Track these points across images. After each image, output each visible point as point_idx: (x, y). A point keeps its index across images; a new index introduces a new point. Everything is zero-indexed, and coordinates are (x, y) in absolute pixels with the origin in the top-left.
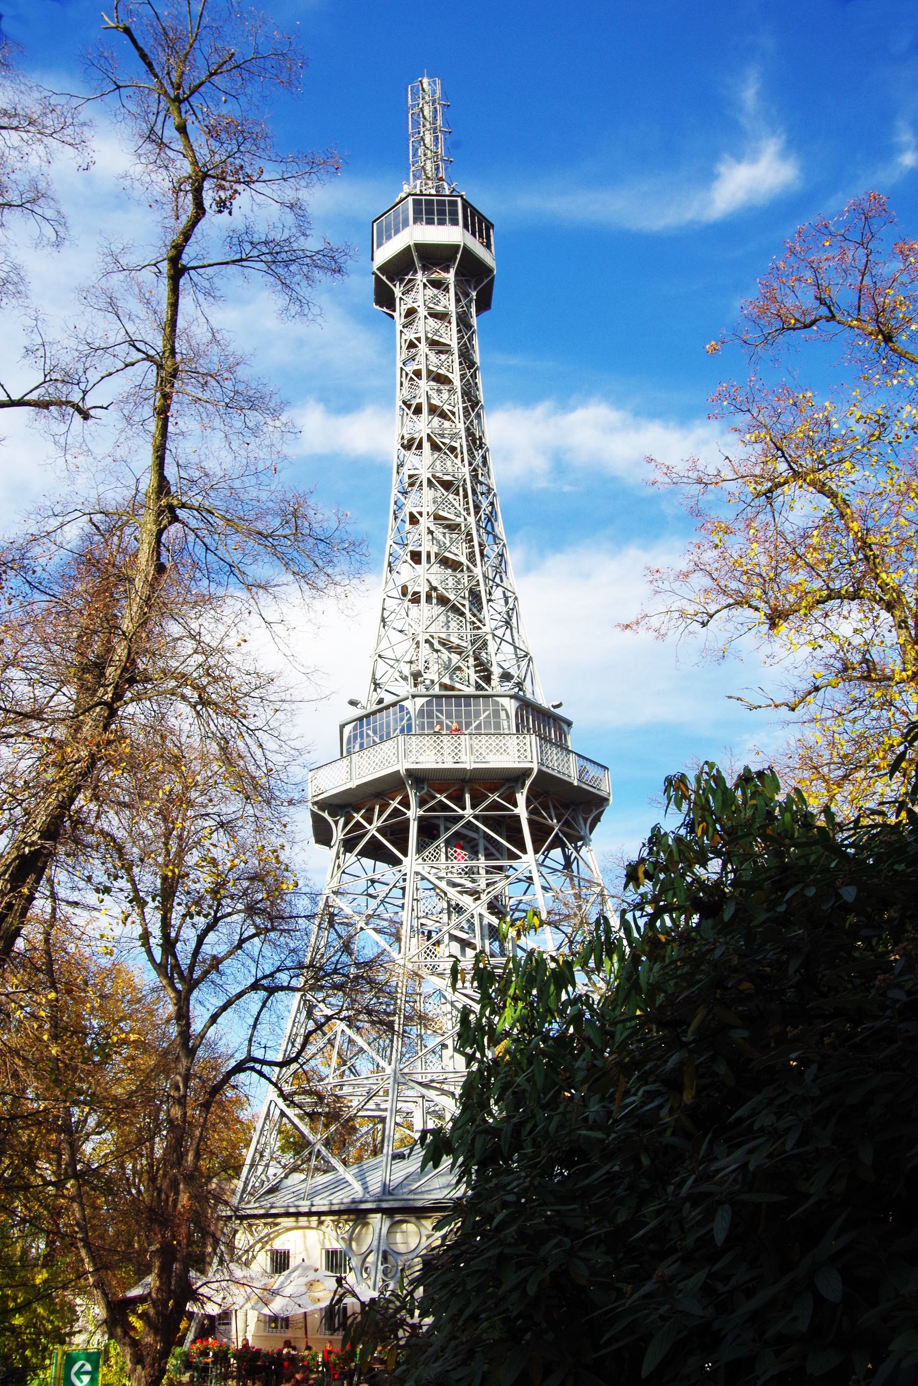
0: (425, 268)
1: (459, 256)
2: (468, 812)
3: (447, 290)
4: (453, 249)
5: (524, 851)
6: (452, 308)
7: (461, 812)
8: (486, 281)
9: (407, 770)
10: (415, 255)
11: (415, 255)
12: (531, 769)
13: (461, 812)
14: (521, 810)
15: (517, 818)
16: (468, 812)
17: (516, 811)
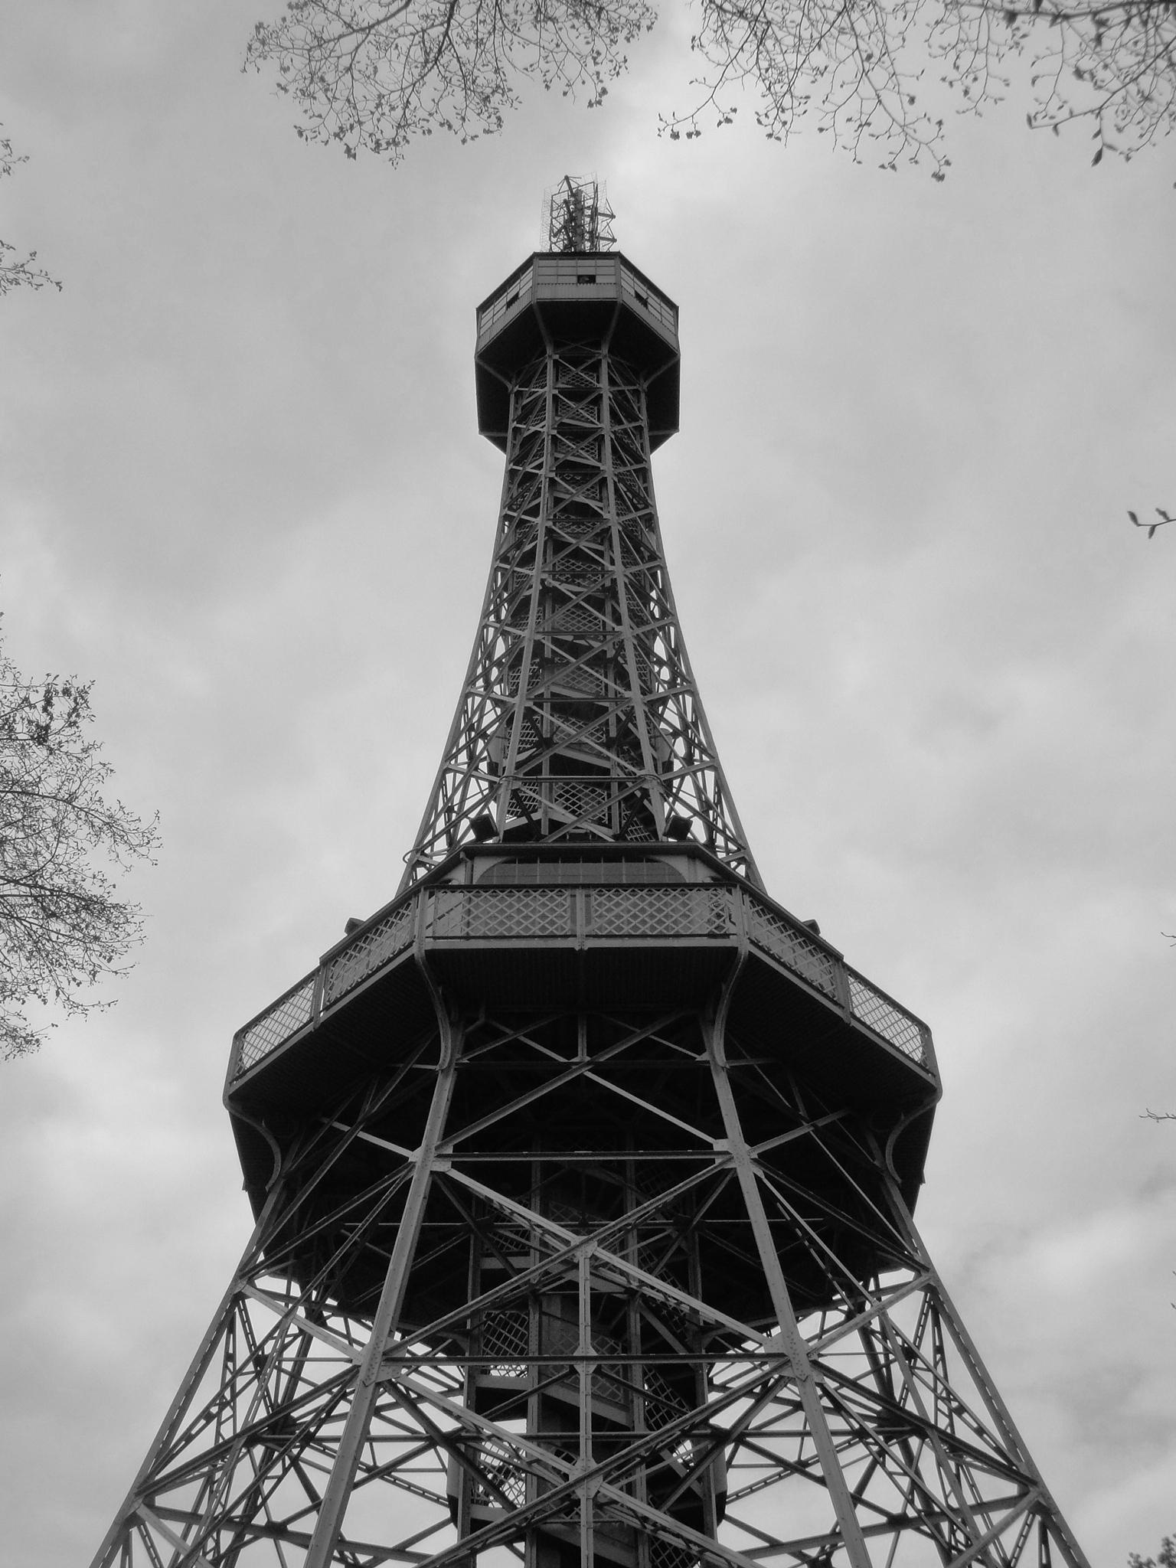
0: (557, 346)
1: (613, 324)
2: (582, 1056)
3: (595, 368)
4: (606, 308)
5: (720, 1133)
6: (604, 385)
7: (562, 1060)
8: (665, 368)
9: (431, 954)
10: (541, 325)
11: (541, 325)
12: (734, 950)
13: (562, 1060)
14: (716, 1053)
15: (704, 1073)
16: (582, 1056)
17: (705, 1057)
